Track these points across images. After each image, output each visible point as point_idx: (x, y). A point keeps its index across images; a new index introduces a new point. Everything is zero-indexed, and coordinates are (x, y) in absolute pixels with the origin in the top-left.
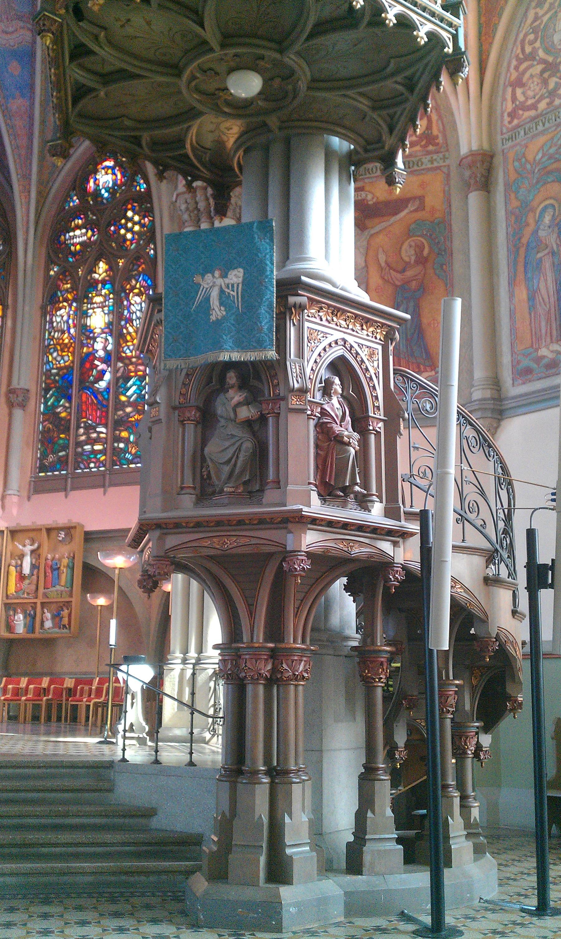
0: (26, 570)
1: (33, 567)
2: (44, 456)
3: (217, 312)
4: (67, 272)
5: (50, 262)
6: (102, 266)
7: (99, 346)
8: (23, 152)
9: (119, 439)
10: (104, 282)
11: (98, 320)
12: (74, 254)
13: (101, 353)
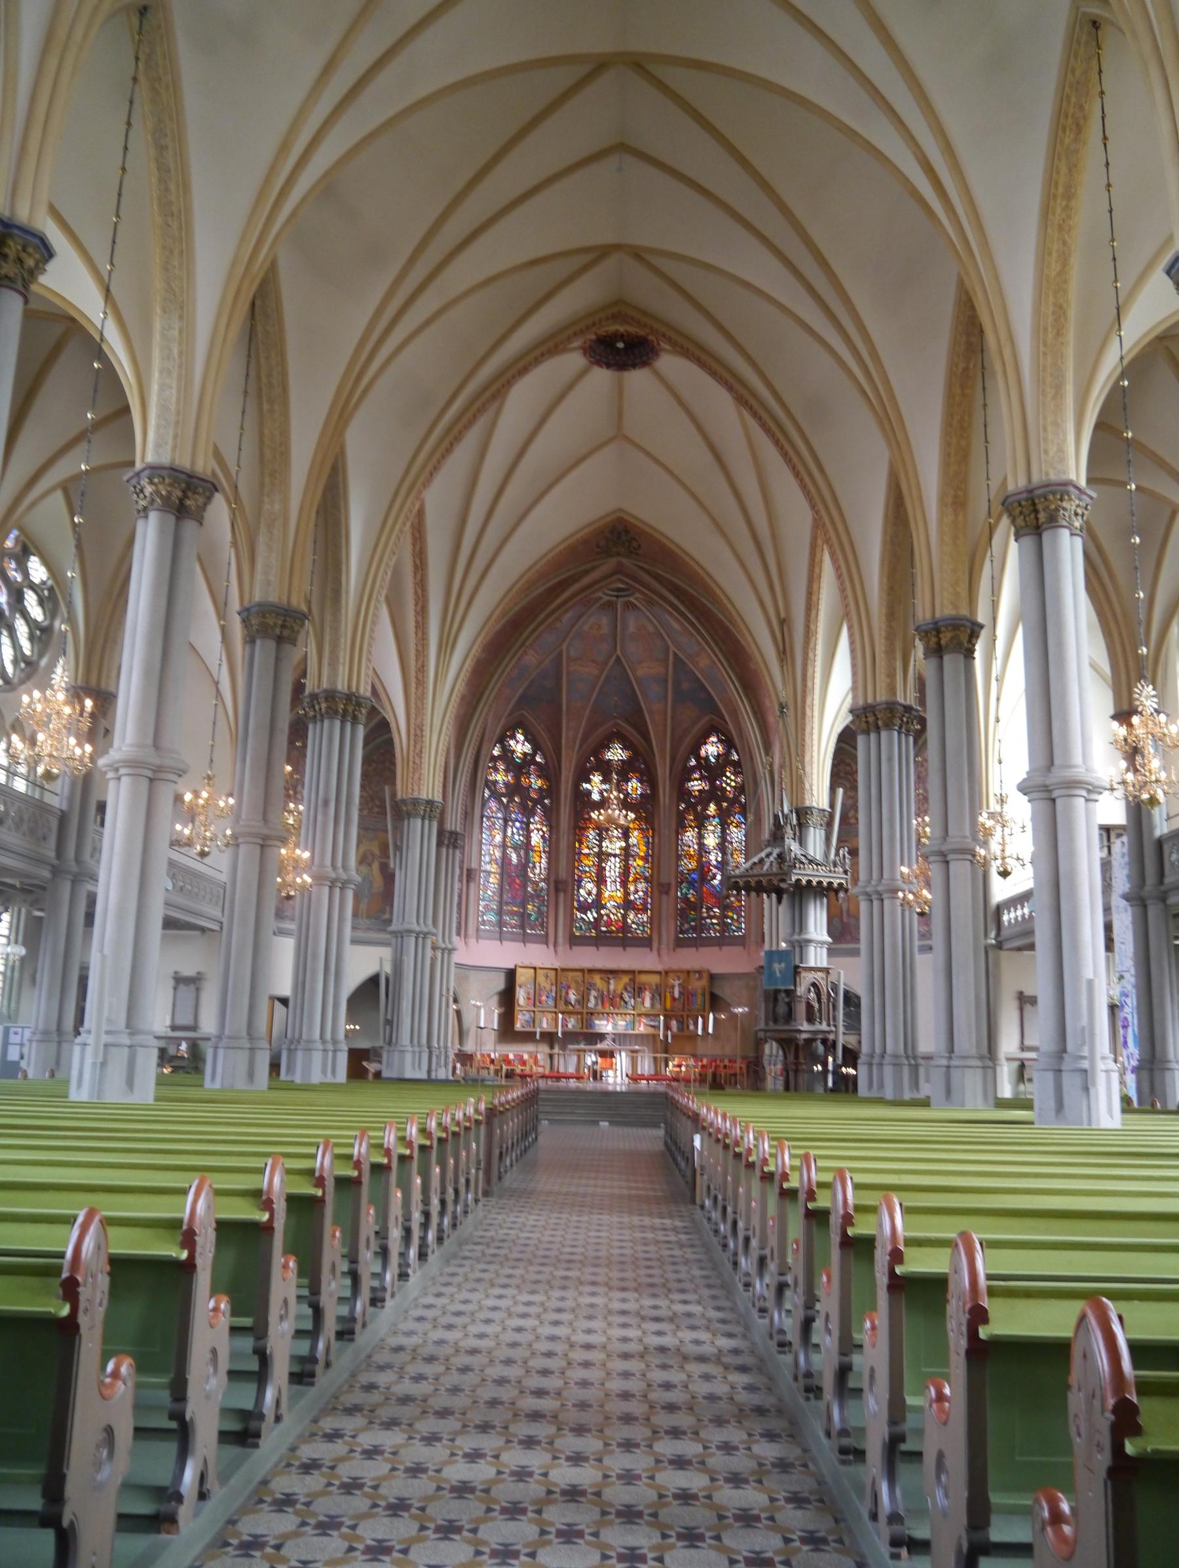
0: (676, 995)
1: (680, 993)
2: (682, 924)
3: (778, 975)
4: (691, 807)
6: (712, 809)
7: (712, 857)
9: (727, 917)
10: (714, 817)
11: (711, 841)
12: (695, 797)
13: (714, 863)
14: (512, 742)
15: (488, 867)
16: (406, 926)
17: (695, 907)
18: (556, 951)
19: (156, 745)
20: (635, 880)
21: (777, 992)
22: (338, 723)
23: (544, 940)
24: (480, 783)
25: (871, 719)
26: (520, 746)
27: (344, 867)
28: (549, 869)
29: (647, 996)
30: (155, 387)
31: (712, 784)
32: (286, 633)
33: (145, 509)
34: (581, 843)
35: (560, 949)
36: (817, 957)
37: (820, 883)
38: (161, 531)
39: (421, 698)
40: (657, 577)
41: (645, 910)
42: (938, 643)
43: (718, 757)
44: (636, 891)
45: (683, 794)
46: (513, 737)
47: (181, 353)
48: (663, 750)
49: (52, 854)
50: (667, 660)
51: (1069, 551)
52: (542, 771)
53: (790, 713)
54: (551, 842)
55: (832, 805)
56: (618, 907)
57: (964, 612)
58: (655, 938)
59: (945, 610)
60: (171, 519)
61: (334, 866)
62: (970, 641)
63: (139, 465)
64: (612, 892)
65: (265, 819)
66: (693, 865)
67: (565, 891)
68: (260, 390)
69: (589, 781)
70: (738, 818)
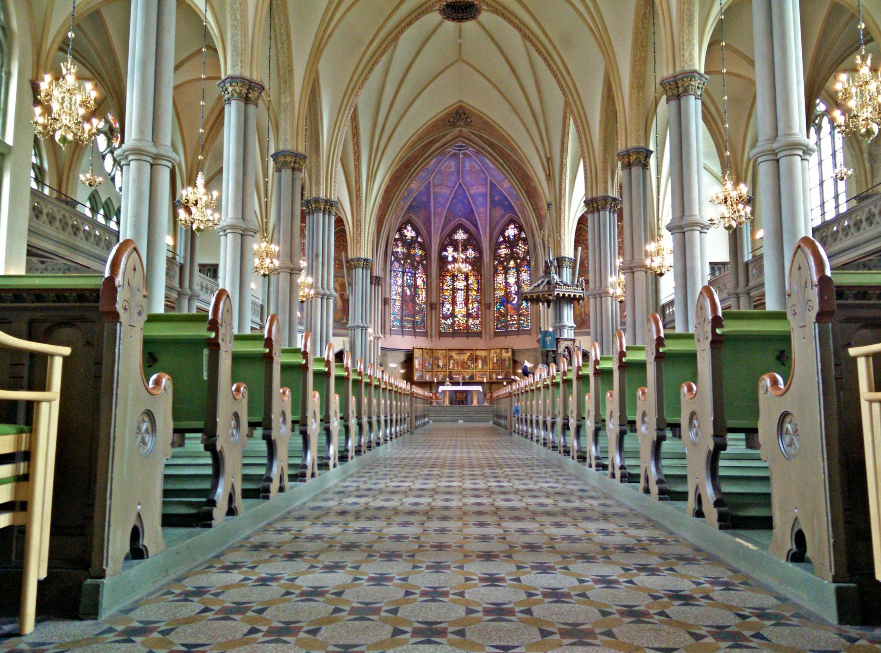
4: (501, 263)
5: (495, 259)
6: (512, 263)
11: (512, 280)
14: (405, 231)
15: (395, 297)
16: (356, 324)
17: (504, 315)
19: (243, 218)
20: (472, 302)
21: (548, 351)
22: (321, 215)
23: (425, 334)
24: (389, 253)
25: (595, 205)
26: (409, 233)
27: (328, 288)
28: (427, 297)
29: (480, 362)
30: (229, 35)
31: (512, 251)
32: (297, 166)
33: (229, 99)
34: (443, 284)
35: (434, 339)
36: (568, 334)
37: (569, 295)
38: (238, 111)
39: (359, 205)
40: (481, 138)
41: (478, 317)
42: (629, 162)
43: (515, 235)
45: (496, 256)
46: (406, 228)
47: (241, 16)
48: (485, 233)
49: (177, 285)
50: (486, 184)
51: (694, 106)
52: (422, 246)
53: (553, 208)
54: (427, 283)
55: (575, 256)
56: (463, 316)
57: (642, 145)
58: (483, 331)
59: (632, 144)
60: (242, 104)
61: (322, 287)
62: (645, 160)
63: (223, 77)
64: (460, 310)
65: (291, 261)
66: (503, 293)
68: (276, 36)
69: (446, 251)
70: (525, 268)
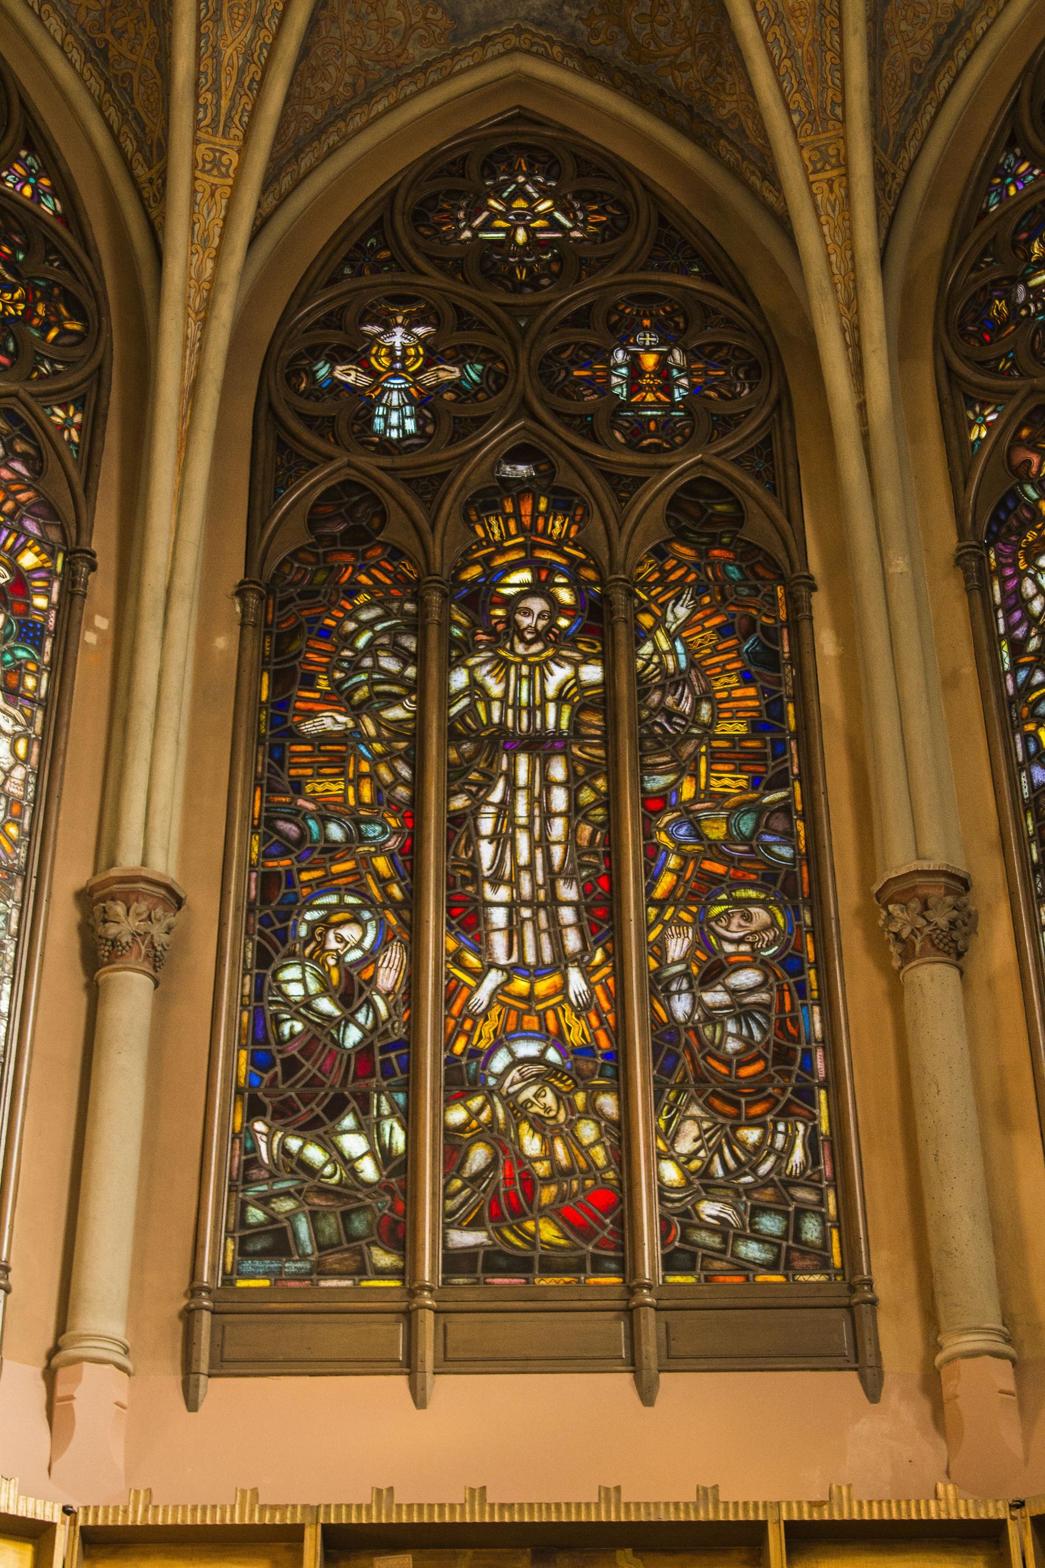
5: (957, 398)
8: (804, 32)
18: (55, 1409)
20: (699, 891)
34: (289, 677)
35: (95, 1390)
44: (714, 971)
48: (822, 117)
67: (159, 963)
69: (356, 353)
